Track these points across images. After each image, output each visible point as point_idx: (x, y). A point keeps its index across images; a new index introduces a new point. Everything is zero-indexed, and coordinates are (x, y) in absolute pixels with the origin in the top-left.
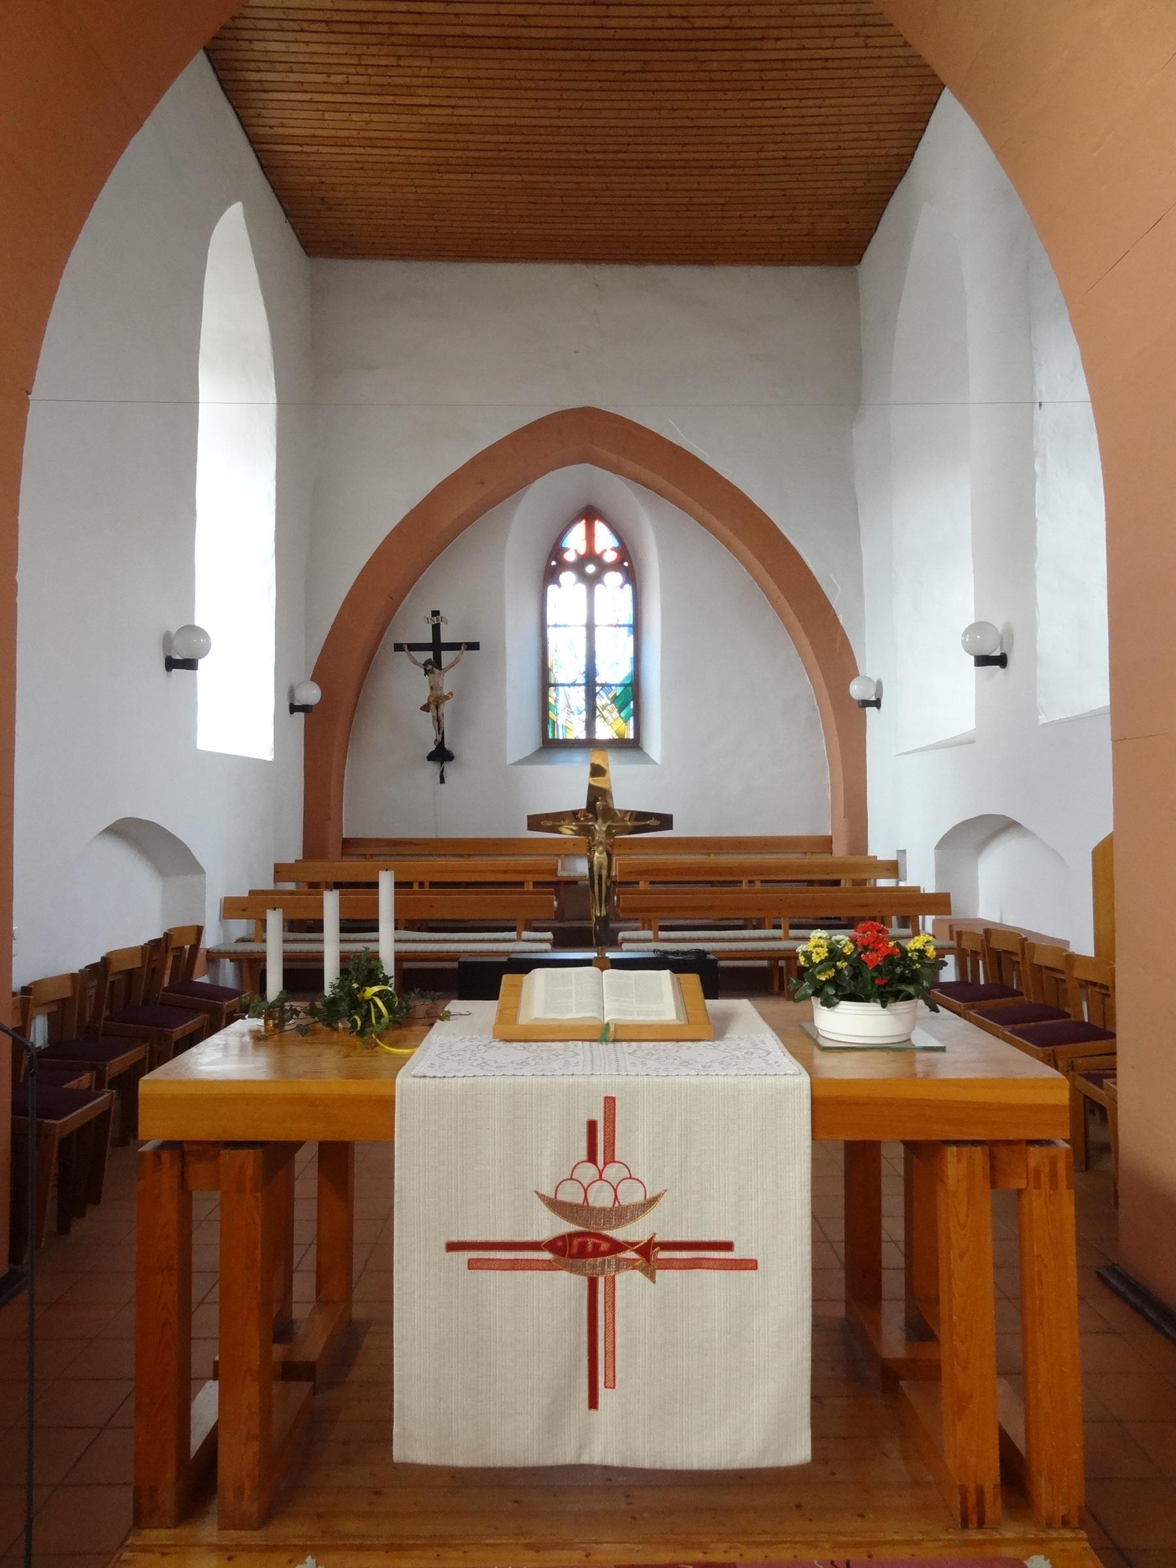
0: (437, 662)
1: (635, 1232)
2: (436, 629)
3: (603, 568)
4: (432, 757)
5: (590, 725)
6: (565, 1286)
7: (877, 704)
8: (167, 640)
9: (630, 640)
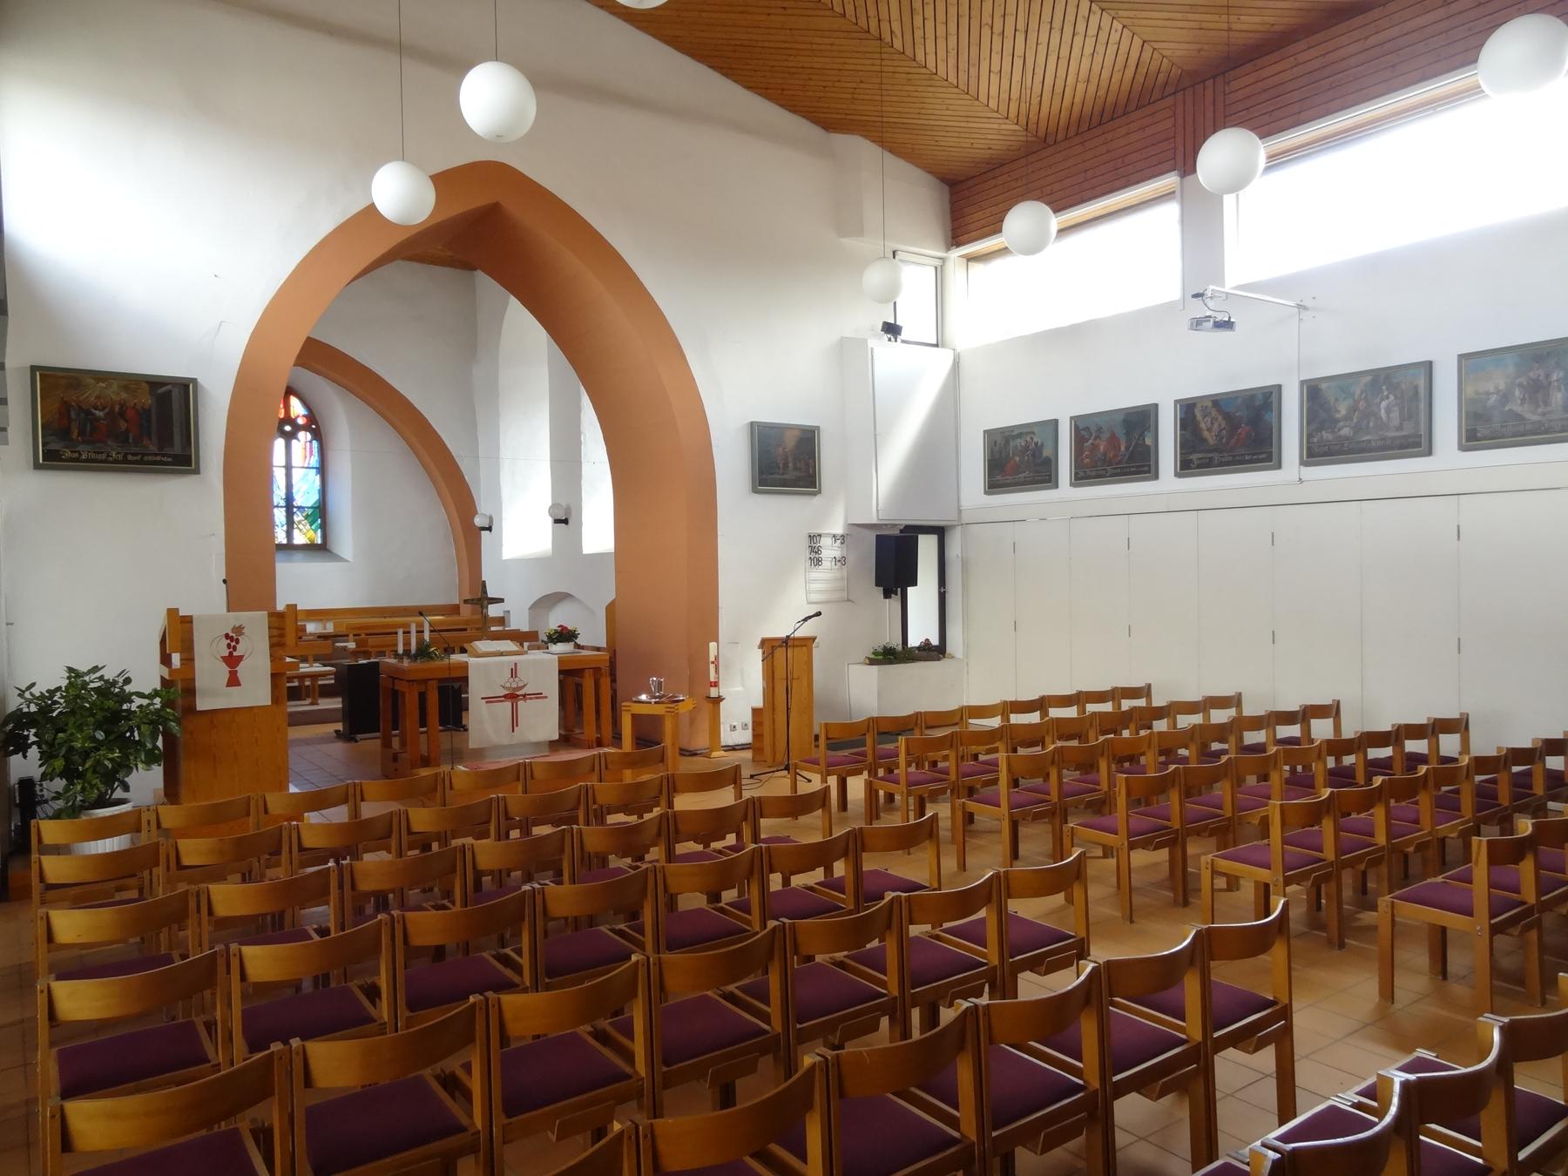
3: (297, 428)
5: (289, 534)
6: (508, 704)
7: (490, 529)
9: (318, 478)
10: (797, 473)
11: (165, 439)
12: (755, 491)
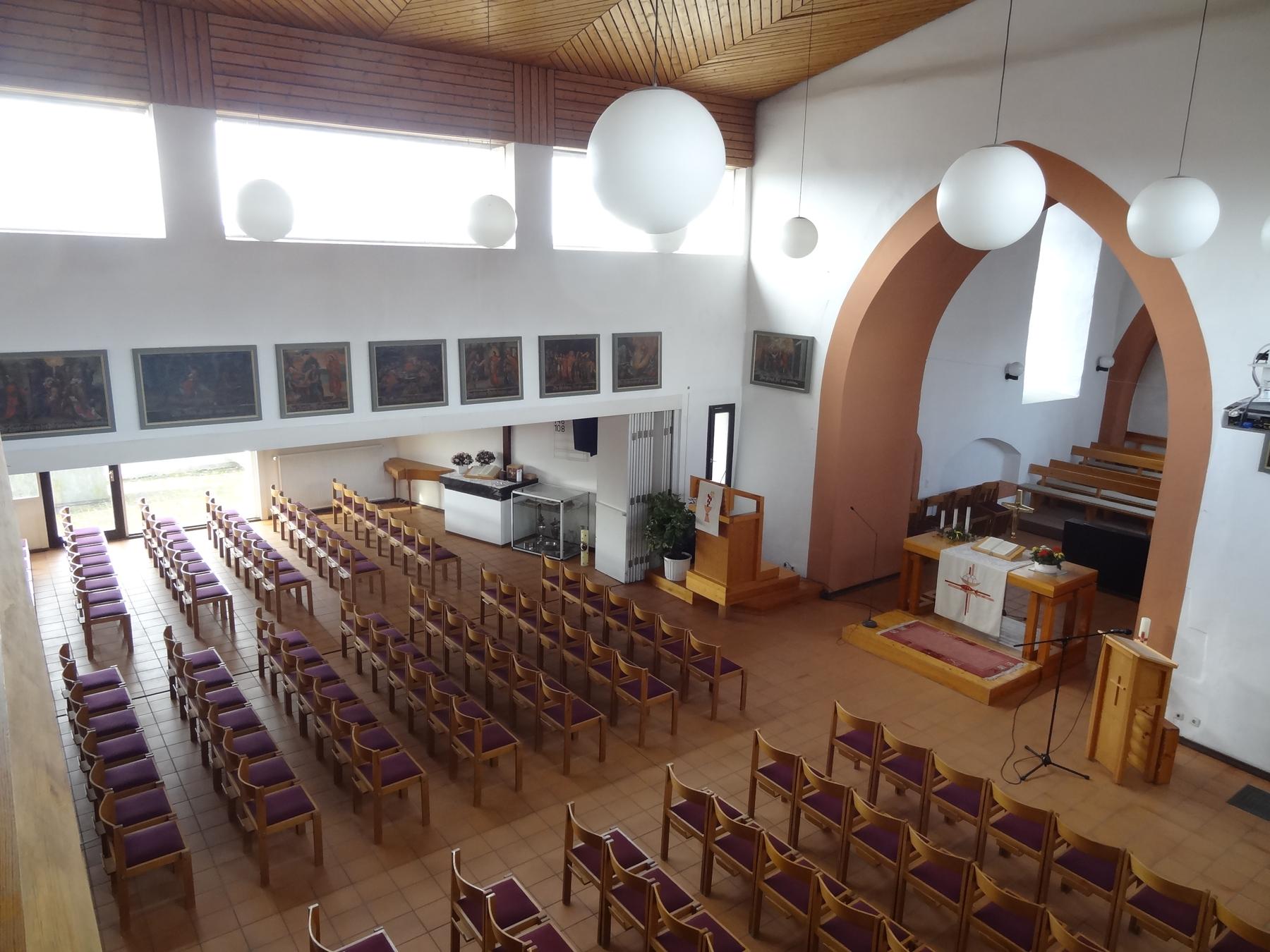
1: (975, 588)
6: (962, 593)
8: (1008, 367)
11: (796, 373)
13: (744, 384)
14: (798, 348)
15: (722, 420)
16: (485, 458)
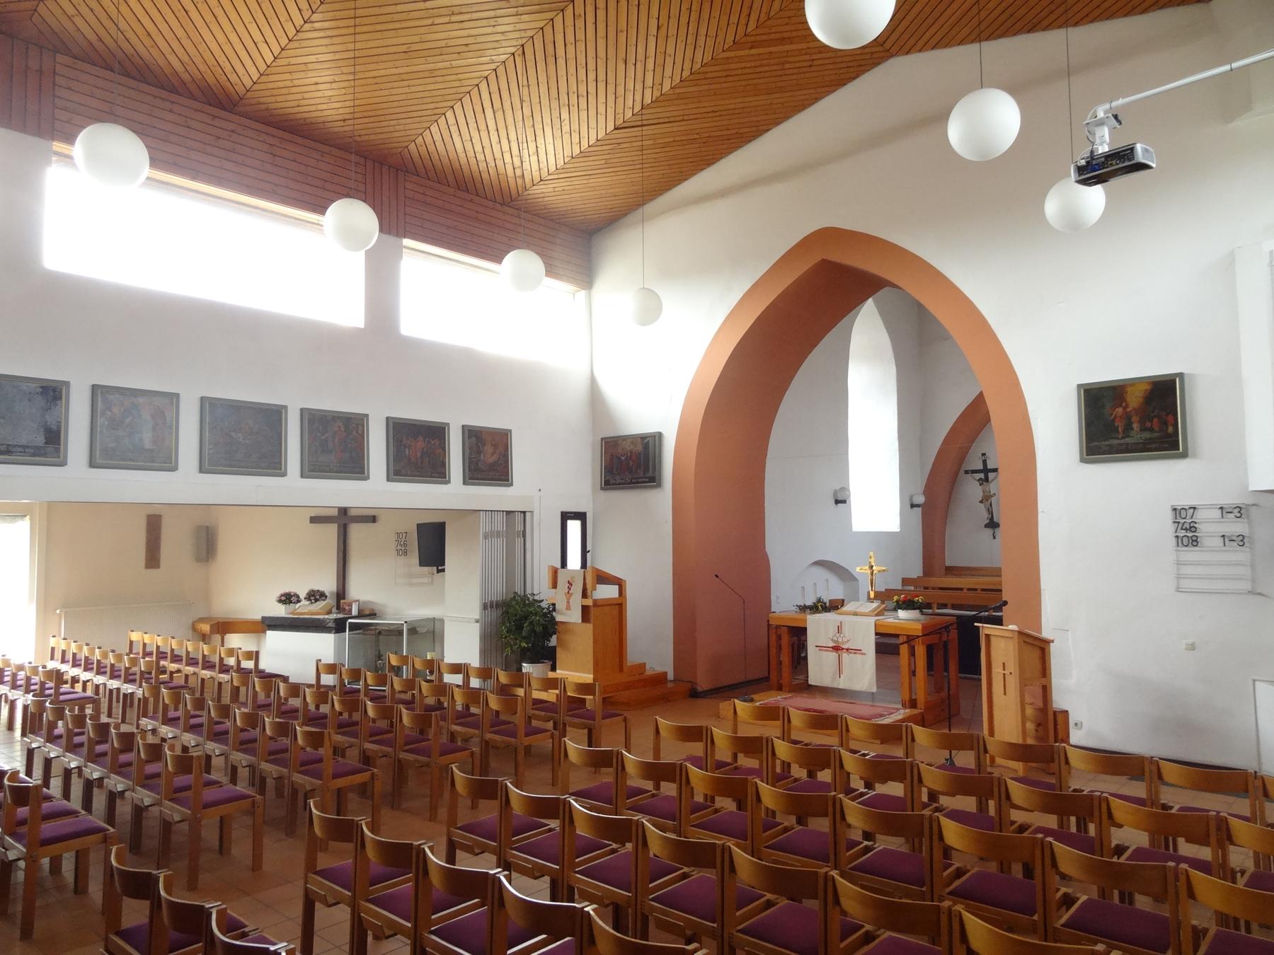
0: (987, 479)
1: (845, 646)
2: (985, 462)
4: (986, 526)
6: (834, 655)
8: (835, 493)
10: (1147, 435)
11: (646, 469)
12: (1083, 460)
13: (594, 492)
14: (646, 446)
15: (574, 527)
16: (315, 596)
